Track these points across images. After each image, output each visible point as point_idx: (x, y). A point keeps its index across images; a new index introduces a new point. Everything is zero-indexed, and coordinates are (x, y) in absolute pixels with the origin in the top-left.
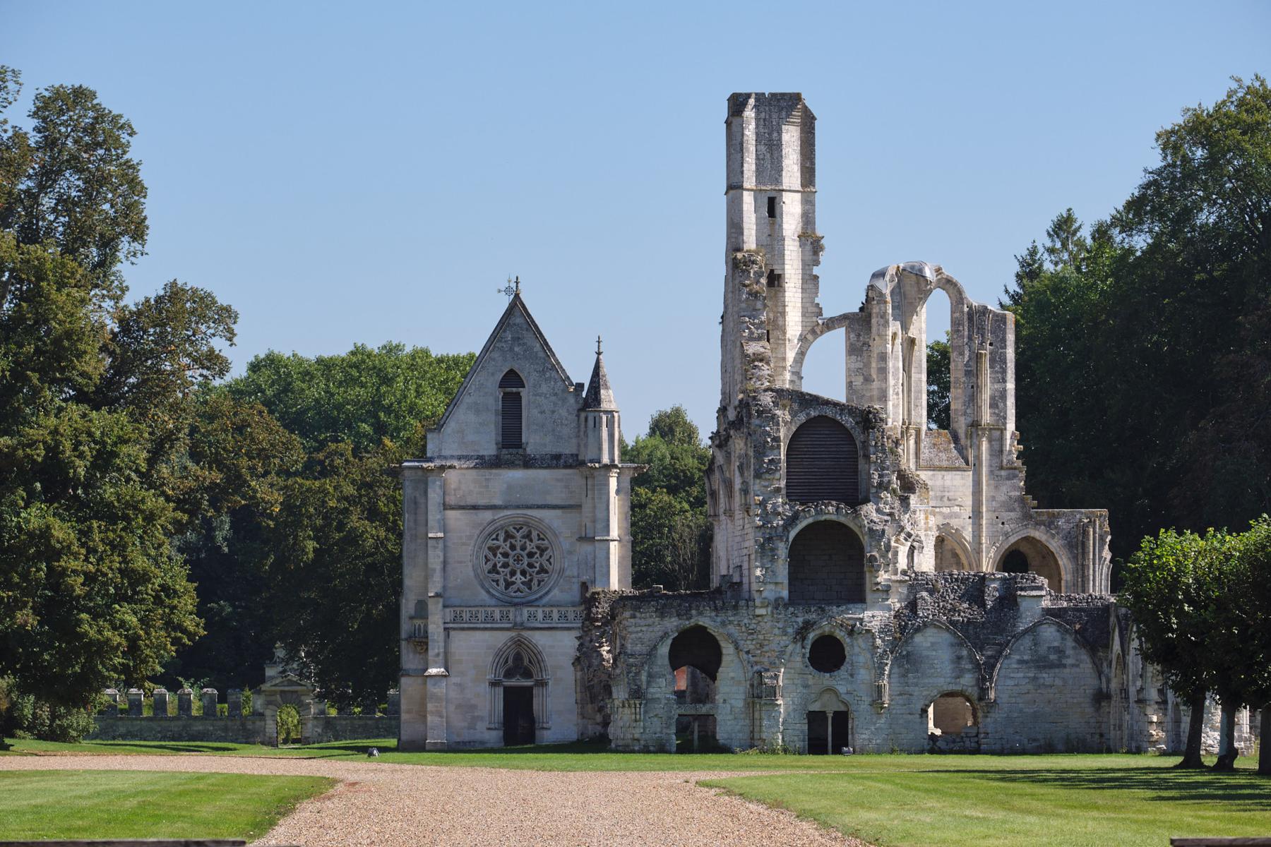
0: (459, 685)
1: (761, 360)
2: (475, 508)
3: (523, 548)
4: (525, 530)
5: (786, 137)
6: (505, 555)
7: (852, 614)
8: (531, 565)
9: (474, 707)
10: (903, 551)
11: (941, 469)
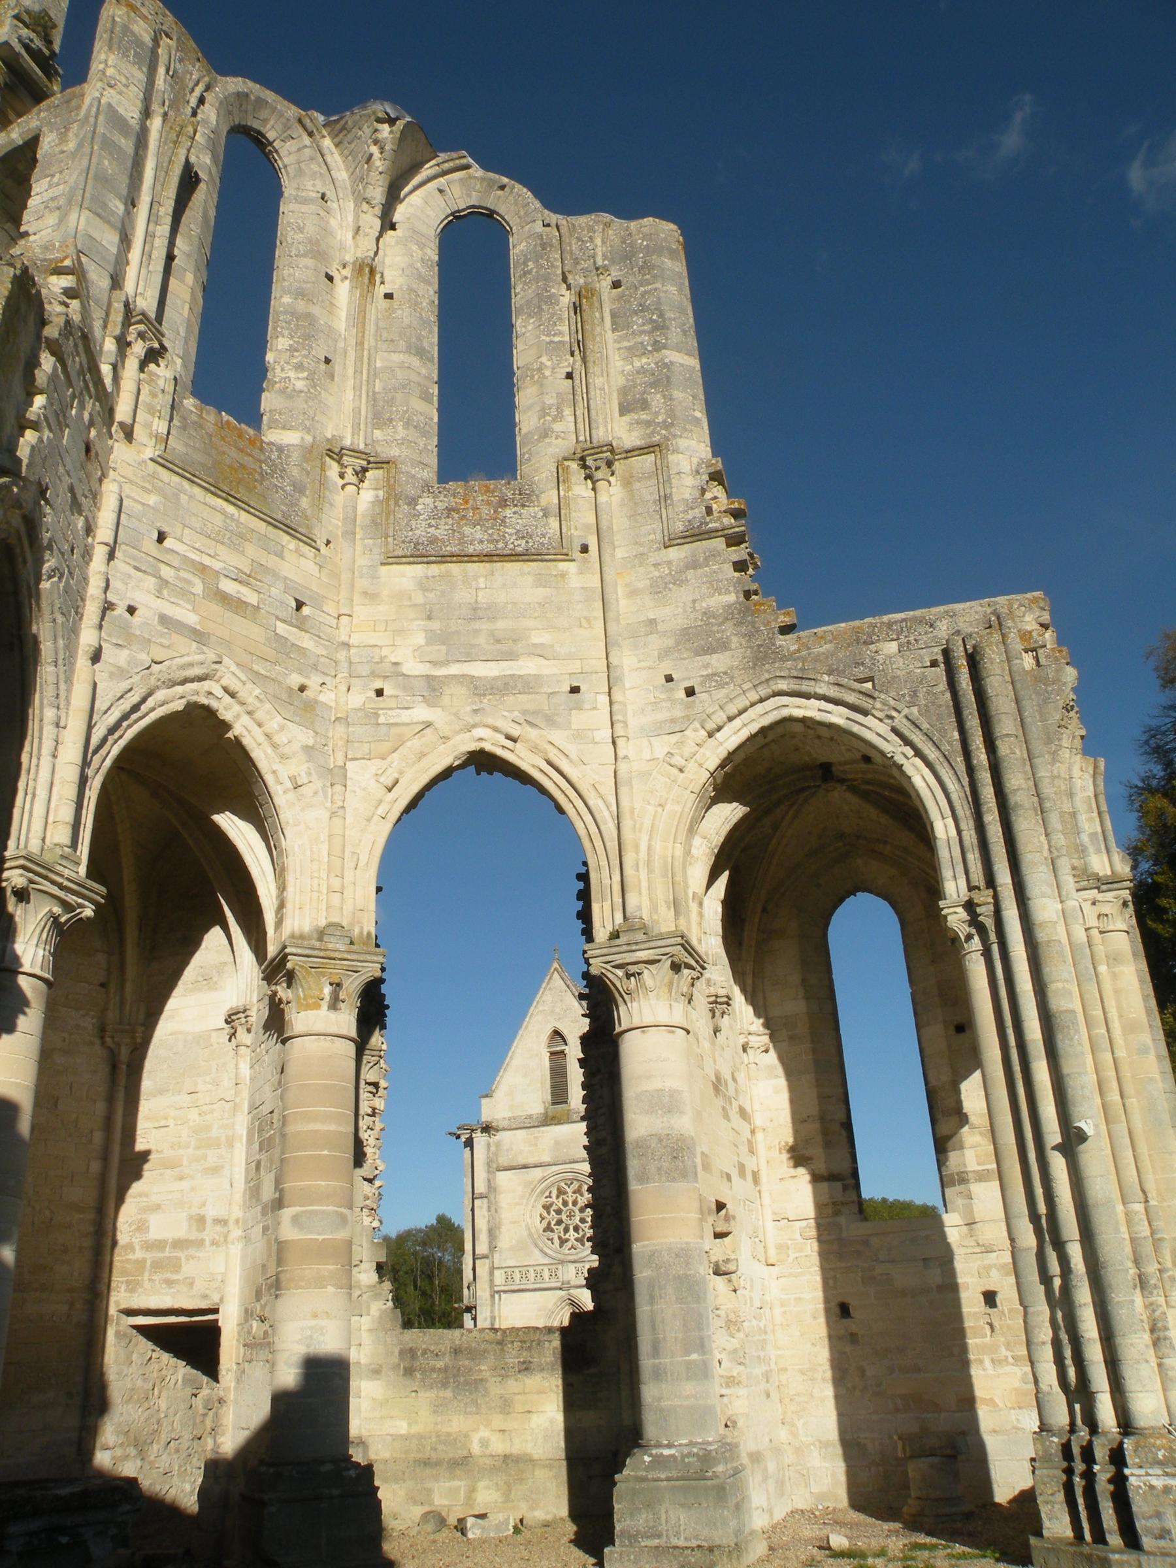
2: (525, 1167)
3: (575, 1203)
4: (575, 1185)
6: (559, 1212)
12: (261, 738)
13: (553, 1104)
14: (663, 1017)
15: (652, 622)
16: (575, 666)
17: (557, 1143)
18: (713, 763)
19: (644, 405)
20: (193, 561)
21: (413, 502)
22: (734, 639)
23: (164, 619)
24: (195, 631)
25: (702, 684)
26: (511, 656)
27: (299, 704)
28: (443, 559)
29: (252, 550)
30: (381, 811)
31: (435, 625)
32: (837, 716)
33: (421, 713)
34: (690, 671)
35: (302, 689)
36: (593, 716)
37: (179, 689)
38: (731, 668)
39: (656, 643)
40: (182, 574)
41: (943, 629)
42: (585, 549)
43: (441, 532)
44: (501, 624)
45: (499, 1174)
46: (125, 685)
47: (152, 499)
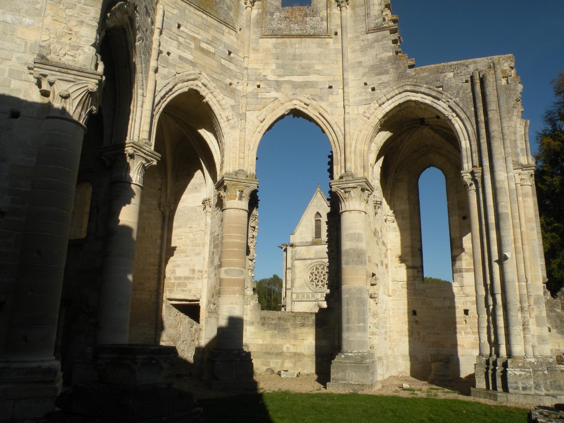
2: (305, 259)
3: (322, 272)
4: (322, 267)
6: (316, 275)
12: (216, 102)
14: (357, 207)
15: (361, 62)
16: (331, 78)
17: (316, 252)
18: (380, 116)
20: (191, 36)
21: (272, 14)
22: (391, 70)
23: (180, 57)
24: (192, 62)
25: (378, 86)
26: (307, 74)
27: (229, 89)
28: (283, 36)
29: (212, 32)
30: (258, 130)
31: (280, 62)
32: (428, 100)
33: (274, 94)
34: (373, 81)
35: (231, 84)
36: (337, 97)
37: (186, 83)
38: (389, 81)
39: (361, 70)
40: (187, 40)
41: (472, 68)
42: (336, 34)
43: (282, 26)
44: (304, 62)
45: (296, 262)
46: (167, 81)
47: (176, 12)
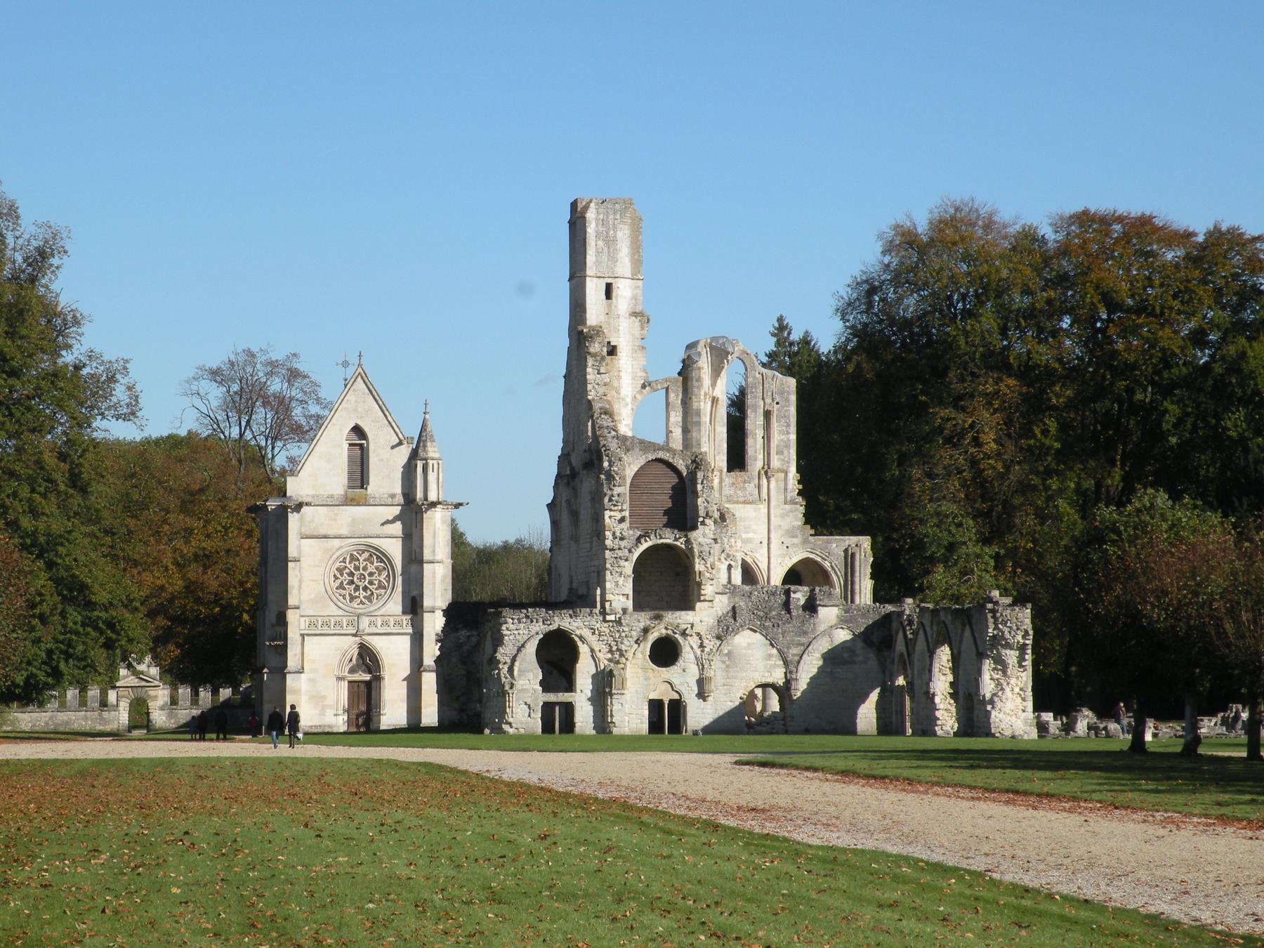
0: (312, 680)
1: (606, 413)
2: (325, 537)
3: (365, 569)
4: (366, 555)
5: (619, 234)
7: (683, 618)
8: (371, 583)
9: (324, 697)
10: (724, 567)
11: (738, 502)
13: (350, 487)
19: (782, 453)
32: (819, 559)
39: (781, 532)
